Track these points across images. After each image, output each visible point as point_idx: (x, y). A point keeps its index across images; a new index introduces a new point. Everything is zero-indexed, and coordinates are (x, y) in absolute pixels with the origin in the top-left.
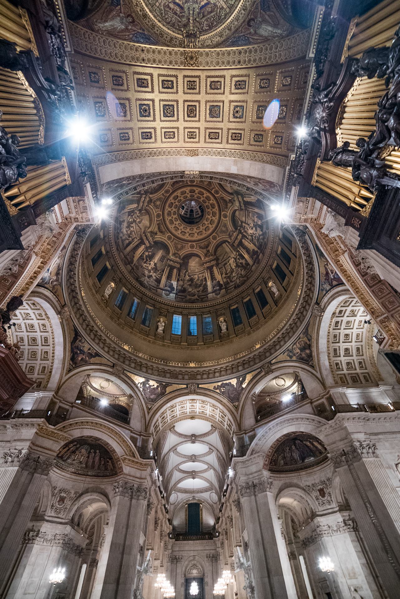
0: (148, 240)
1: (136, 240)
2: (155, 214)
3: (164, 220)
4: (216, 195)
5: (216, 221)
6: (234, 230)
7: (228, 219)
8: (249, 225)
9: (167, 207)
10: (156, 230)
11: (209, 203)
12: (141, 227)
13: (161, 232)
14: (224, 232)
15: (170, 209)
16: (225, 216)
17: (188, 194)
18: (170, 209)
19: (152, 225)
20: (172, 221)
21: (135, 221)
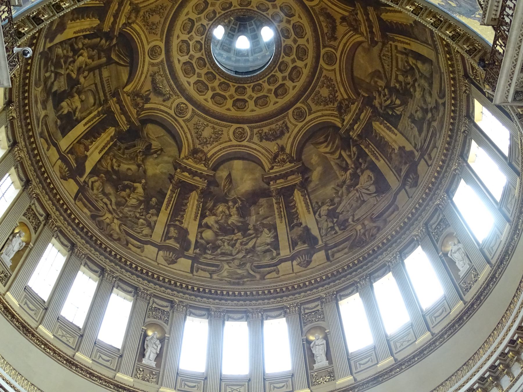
0: (368, 20)
1: (400, 46)
2: (337, 66)
3: (317, 41)
4: (183, 100)
5: (177, 31)
6: (128, 30)
7: (147, 48)
8: (91, 70)
9: (306, 72)
10: (341, 29)
11: (199, 75)
12: (378, 61)
13: (329, 17)
14: (153, 12)
15: (299, 63)
16: (154, 52)
17: (251, 97)
18: (299, 63)
19: (349, 45)
20: (296, 34)
21: (387, 86)
